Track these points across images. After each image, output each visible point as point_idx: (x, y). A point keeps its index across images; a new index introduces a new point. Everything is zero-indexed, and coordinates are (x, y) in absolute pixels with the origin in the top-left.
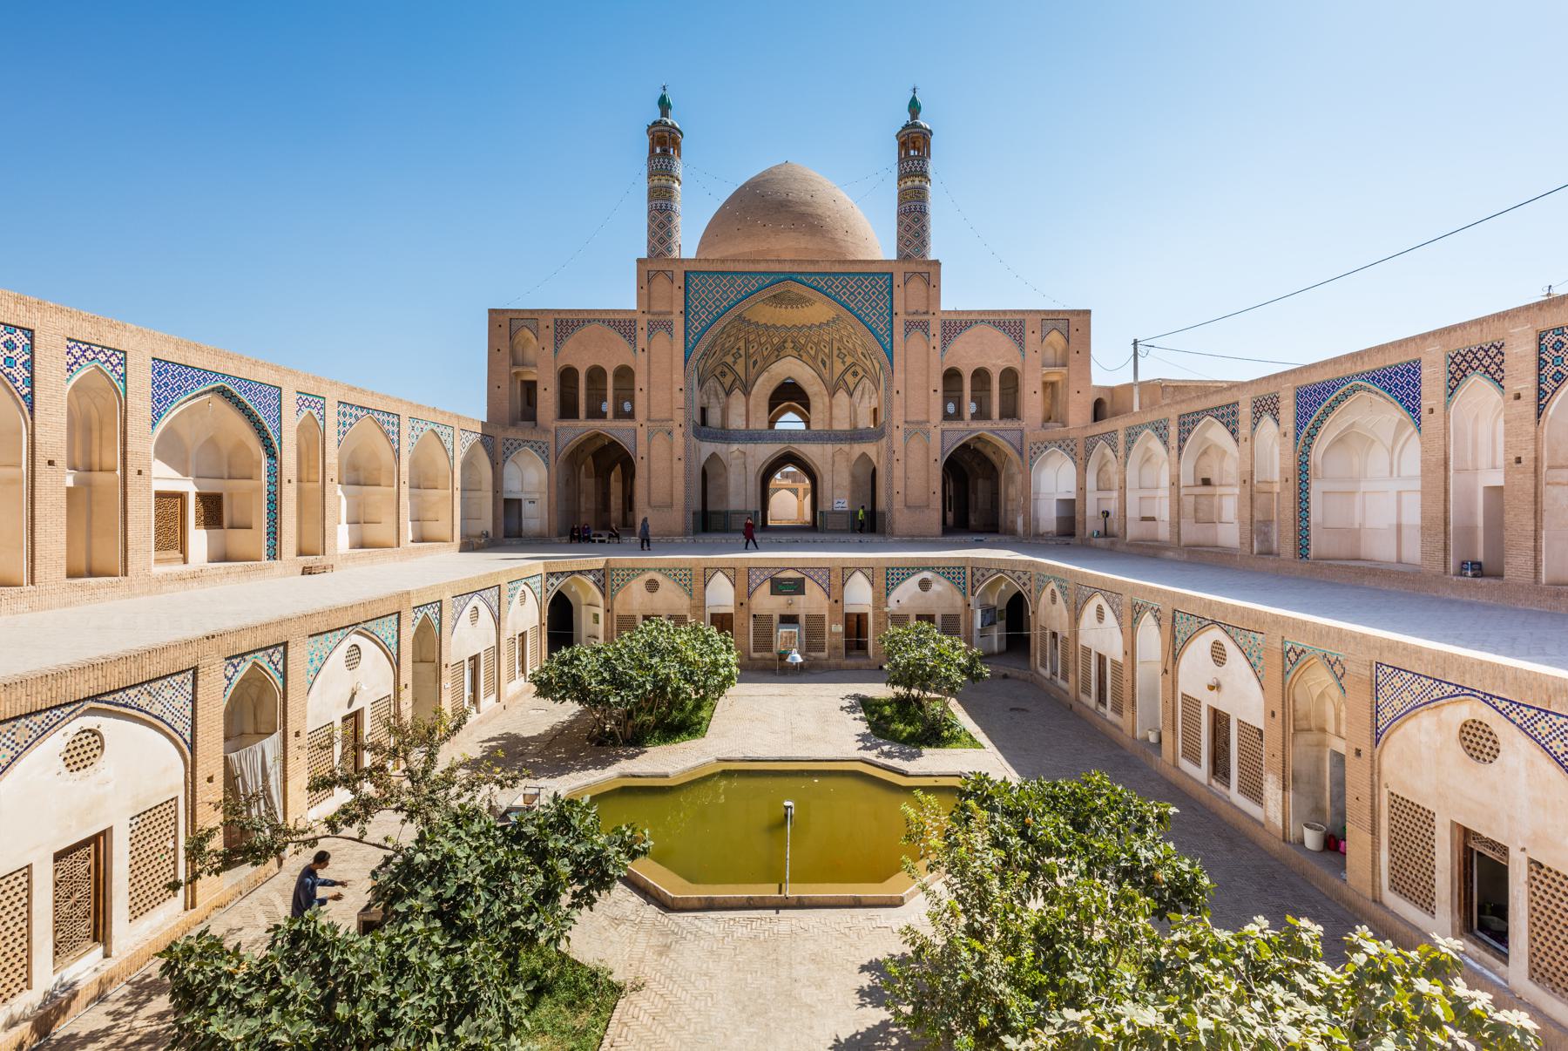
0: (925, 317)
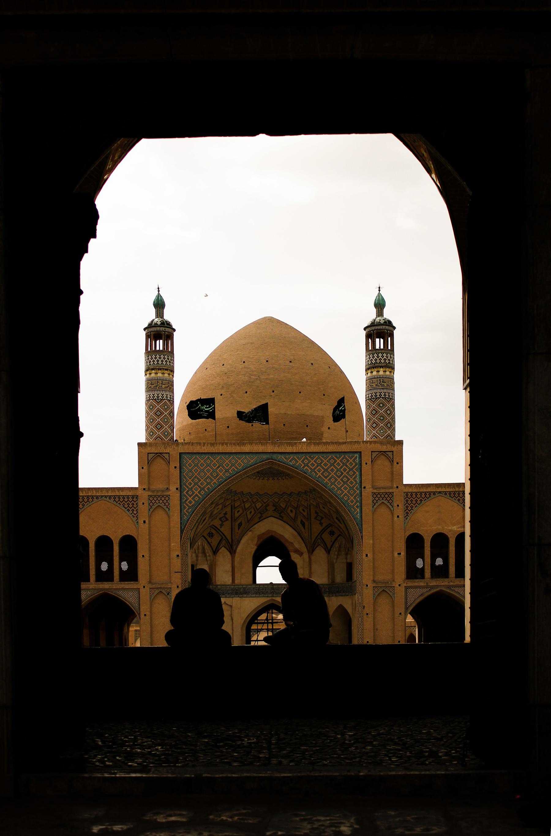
0: (391, 491)
